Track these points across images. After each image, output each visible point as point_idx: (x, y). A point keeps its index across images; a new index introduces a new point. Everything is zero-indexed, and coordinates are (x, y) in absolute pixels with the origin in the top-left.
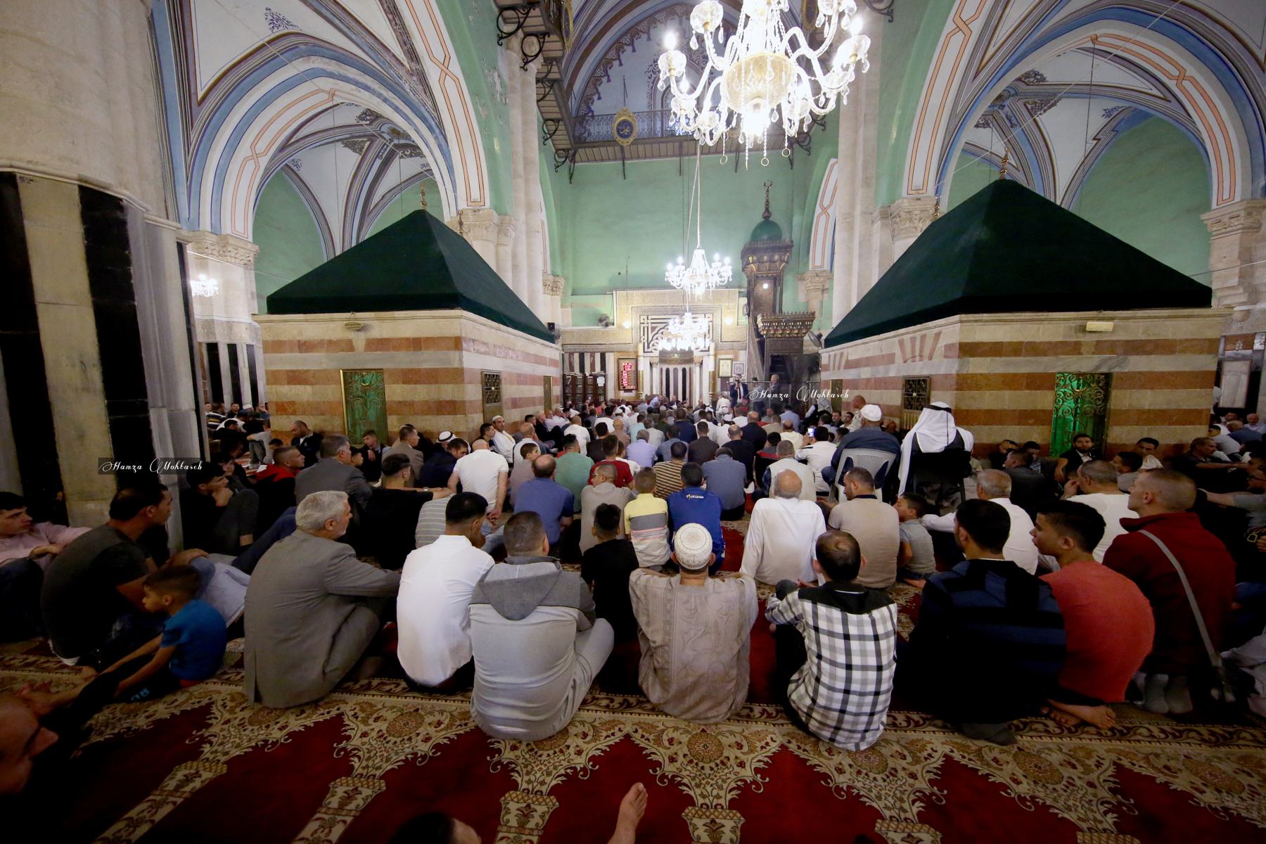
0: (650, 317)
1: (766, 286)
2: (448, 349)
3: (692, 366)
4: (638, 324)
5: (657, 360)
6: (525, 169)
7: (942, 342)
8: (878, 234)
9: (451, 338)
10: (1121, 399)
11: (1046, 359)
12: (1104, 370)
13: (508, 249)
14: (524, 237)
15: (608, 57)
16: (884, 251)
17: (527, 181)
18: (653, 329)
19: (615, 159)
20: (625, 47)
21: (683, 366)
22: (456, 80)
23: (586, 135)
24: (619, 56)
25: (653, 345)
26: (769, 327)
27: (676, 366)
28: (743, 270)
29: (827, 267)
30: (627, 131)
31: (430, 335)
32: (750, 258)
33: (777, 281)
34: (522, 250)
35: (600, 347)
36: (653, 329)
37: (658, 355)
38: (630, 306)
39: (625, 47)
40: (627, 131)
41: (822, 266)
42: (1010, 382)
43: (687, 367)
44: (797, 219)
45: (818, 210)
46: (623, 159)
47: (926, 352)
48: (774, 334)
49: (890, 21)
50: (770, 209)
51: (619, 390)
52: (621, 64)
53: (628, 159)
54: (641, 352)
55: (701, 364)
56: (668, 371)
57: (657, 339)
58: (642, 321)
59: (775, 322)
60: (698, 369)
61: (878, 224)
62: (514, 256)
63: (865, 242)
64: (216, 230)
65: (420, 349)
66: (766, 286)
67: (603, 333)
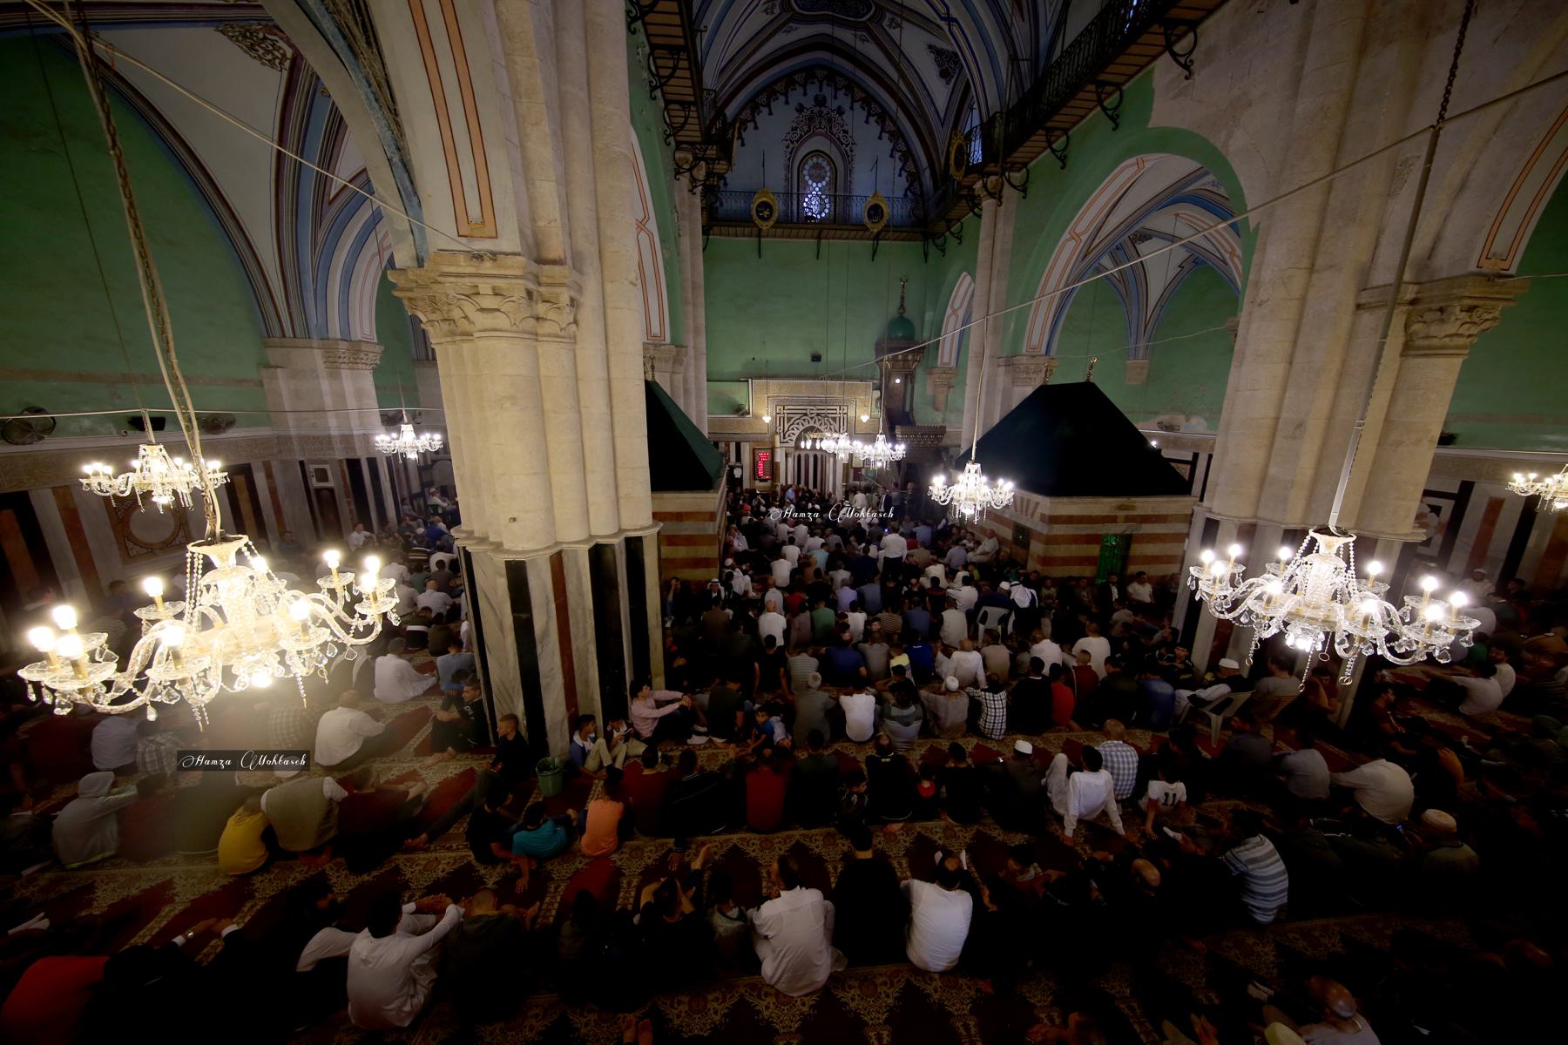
1: (898, 381)
2: (704, 520)
6: (693, 293)
7: (1039, 511)
8: (1002, 378)
9: (706, 513)
10: (1137, 549)
11: (1096, 526)
12: (1128, 532)
13: (680, 377)
14: (693, 361)
15: (743, 117)
16: (1007, 395)
17: (694, 305)
18: (789, 419)
19: (750, 236)
20: (761, 108)
22: (650, 235)
23: (718, 204)
24: (754, 117)
29: (953, 364)
30: (766, 213)
31: (690, 510)
33: (909, 377)
34: (692, 373)
35: (736, 436)
36: (789, 419)
39: (761, 108)
40: (766, 213)
41: (949, 363)
42: (1076, 539)
44: (929, 316)
45: (949, 311)
46: (759, 236)
47: (1030, 511)
49: (1024, 197)
50: (905, 305)
51: (755, 479)
52: (756, 128)
53: (764, 237)
54: (778, 444)
56: (799, 457)
61: (1002, 370)
62: (685, 380)
63: (992, 382)
64: (346, 338)
65: (682, 520)
66: (898, 381)
67: (739, 421)
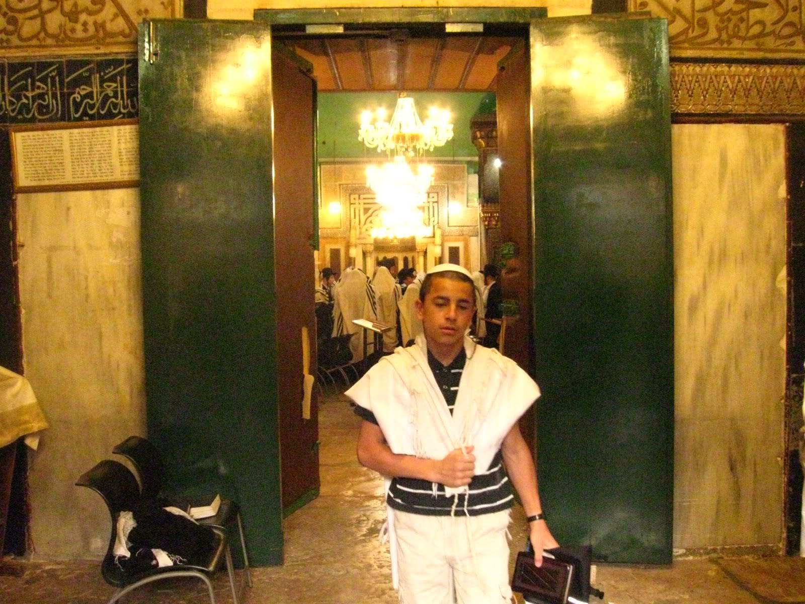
0: (362, 196)
3: (415, 254)
4: (348, 204)
5: (371, 248)
21: (405, 255)
25: (367, 230)
26: (490, 217)
27: (396, 255)
28: (473, 142)
32: (478, 134)
37: (372, 241)
38: (338, 183)
43: (409, 256)
48: (496, 225)
55: (425, 253)
57: (371, 222)
58: (352, 201)
59: (496, 212)
60: (421, 259)
